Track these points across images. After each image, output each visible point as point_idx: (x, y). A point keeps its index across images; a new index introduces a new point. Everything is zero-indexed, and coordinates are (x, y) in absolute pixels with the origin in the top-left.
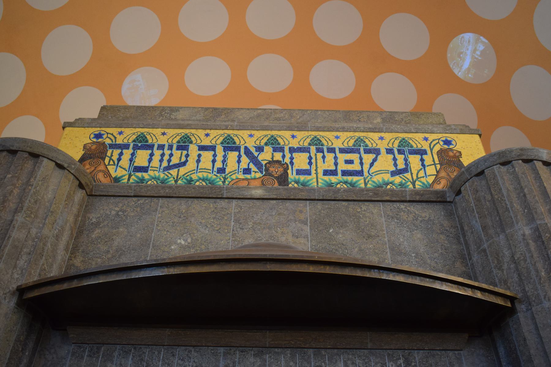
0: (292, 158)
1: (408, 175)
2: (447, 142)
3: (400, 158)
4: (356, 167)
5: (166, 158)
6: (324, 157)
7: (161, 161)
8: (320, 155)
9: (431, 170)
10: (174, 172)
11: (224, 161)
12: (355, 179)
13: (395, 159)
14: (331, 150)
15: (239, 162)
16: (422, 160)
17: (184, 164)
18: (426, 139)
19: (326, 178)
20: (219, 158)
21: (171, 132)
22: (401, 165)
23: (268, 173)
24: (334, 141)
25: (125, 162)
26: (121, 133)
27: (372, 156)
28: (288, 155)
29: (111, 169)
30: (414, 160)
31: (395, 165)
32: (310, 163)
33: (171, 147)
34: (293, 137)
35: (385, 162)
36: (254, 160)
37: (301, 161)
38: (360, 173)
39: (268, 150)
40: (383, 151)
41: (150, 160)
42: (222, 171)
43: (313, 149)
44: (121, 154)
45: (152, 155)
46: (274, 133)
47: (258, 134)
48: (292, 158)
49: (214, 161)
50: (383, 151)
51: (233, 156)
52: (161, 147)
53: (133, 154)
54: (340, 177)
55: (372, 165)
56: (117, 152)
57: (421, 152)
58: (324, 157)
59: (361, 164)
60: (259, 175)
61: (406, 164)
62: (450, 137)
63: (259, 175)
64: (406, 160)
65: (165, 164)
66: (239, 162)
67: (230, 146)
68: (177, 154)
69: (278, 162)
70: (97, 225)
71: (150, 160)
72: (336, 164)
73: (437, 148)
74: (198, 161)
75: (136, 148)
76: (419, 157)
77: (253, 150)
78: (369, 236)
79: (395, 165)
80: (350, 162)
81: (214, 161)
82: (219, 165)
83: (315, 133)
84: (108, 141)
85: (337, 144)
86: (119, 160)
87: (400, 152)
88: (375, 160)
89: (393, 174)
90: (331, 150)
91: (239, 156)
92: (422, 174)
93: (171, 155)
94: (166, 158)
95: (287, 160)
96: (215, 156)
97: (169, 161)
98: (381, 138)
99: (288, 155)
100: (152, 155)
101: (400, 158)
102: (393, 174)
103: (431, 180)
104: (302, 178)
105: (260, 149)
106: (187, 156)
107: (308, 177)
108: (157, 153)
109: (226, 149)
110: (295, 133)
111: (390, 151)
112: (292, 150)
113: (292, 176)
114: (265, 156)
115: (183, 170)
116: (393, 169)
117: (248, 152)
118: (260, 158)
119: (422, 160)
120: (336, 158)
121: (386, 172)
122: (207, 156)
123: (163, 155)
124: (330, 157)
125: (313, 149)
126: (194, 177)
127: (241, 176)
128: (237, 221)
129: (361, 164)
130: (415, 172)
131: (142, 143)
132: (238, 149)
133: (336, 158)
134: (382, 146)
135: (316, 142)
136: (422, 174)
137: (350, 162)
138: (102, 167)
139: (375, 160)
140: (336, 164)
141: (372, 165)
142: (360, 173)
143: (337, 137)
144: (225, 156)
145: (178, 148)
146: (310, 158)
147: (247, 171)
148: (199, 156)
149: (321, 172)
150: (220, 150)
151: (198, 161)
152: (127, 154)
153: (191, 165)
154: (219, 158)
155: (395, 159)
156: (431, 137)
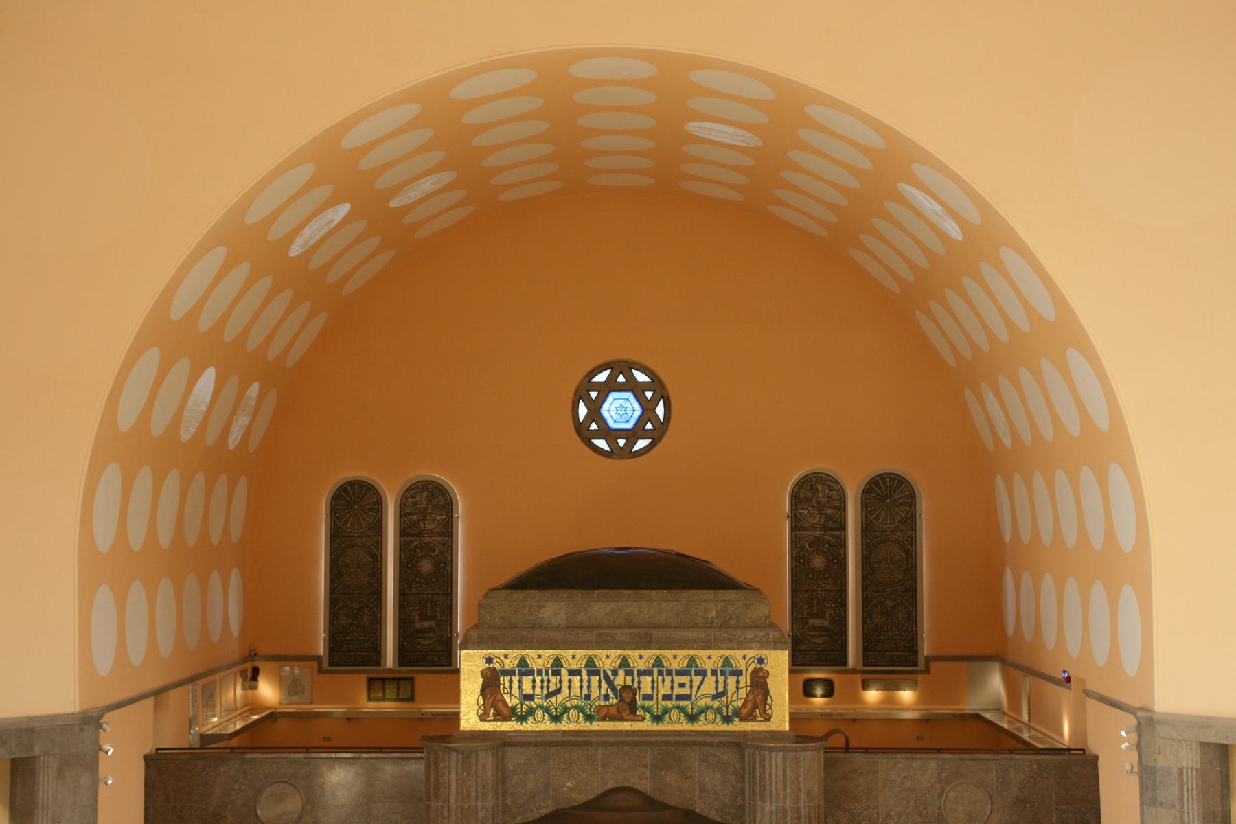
0: (639, 682)
1: (724, 699)
2: (761, 661)
3: (721, 679)
4: (686, 691)
5: (545, 684)
6: (663, 680)
7: (542, 688)
8: (660, 678)
9: (742, 693)
10: (553, 699)
11: (589, 687)
12: (684, 703)
13: (717, 682)
14: (669, 673)
15: (600, 687)
16: (738, 682)
17: (558, 691)
18: (744, 657)
19: (664, 703)
20: (585, 684)
21: (547, 653)
22: (721, 689)
23: (622, 700)
24: (673, 661)
25: (515, 690)
26: (506, 657)
27: (700, 678)
28: (636, 679)
29: (507, 698)
30: (732, 681)
31: (717, 688)
32: (653, 688)
33: (547, 674)
34: (641, 657)
35: (709, 686)
36: (611, 685)
37: (646, 688)
38: (688, 697)
39: (621, 672)
40: (709, 672)
41: (534, 687)
42: (588, 697)
43: (656, 670)
44: (511, 681)
45: (534, 681)
46: (627, 652)
47: (614, 653)
48: (639, 682)
49: (581, 687)
50: (709, 672)
51: (595, 679)
52: (540, 672)
53: (520, 681)
54: (674, 702)
55: (699, 688)
56: (507, 678)
57: (738, 673)
58: (663, 680)
59: (691, 687)
60: (615, 701)
61: (725, 687)
62: (766, 653)
63: (615, 701)
64: (725, 682)
65: (545, 692)
66: (600, 687)
67: (593, 670)
68: (553, 679)
69: (629, 686)
70: (514, 772)
71: (534, 687)
72: (672, 688)
73: (751, 669)
74: (570, 687)
75: (522, 674)
76: (735, 678)
77: (609, 673)
78: (687, 778)
79: (717, 688)
80: (682, 685)
81: (581, 687)
82: (585, 691)
83: (657, 652)
84: (497, 666)
85: (675, 665)
86: (511, 687)
87: (723, 673)
88: (702, 683)
89: (715, 697)
90: (669, 673)
91: (600, 681)
92: (735, 697)
93: (549, 681)
94: (545, 684)
95: (636, 685)
96: (581, 681)
97: (548, 688)
98: (709, 657)
99: (636, 679)
100: (534, 681)
101: (721, 679)
102: (715, 697)
103: (740, 703)
104: (647, 703)
105: (615, 673)
106: (561, 681)
107: (651, 703)
108: (538, 679)
109: (590, 673)
110: (643, 652)
111: (714, 672)
112: (640, 673)
113: (639, 702)
114: (620, 680)
115: (560, 698)
116: (714, 692)
117: (606, 677)
118: (616, 683)
119: (738, 682)
120: (672, 681)
121: (707, 695)
122: (576, 679)
123: (542, 681)
124: (668, 679)
125: (656, 670)
126: (568, 704)
127: (603, 703)
128: (603, 766)
129: (691, 687)
130: (730, 694)
131: (524, 669)
132: (597, 673)
133: (672, 681)
134: (709, 666)
135: (658, 663)
136: (735, 697)
137: (682, 685)
138: (499, 697)
139: (702, 683)
140: (672, 688)
141: (699, 688)
142: (688, 697)
143: (675, 657)
144: (589, 681)
145: (553, 674)
146: (653, 682)
147: (606, 697)
148: (570, 681)
149: (660, 697)
150: (584, 673)
151: (570, 687)
152: (516, 679)
153: (565, 691)
154: (585, 684)
155: (717, 682)
156: (751, 653)
